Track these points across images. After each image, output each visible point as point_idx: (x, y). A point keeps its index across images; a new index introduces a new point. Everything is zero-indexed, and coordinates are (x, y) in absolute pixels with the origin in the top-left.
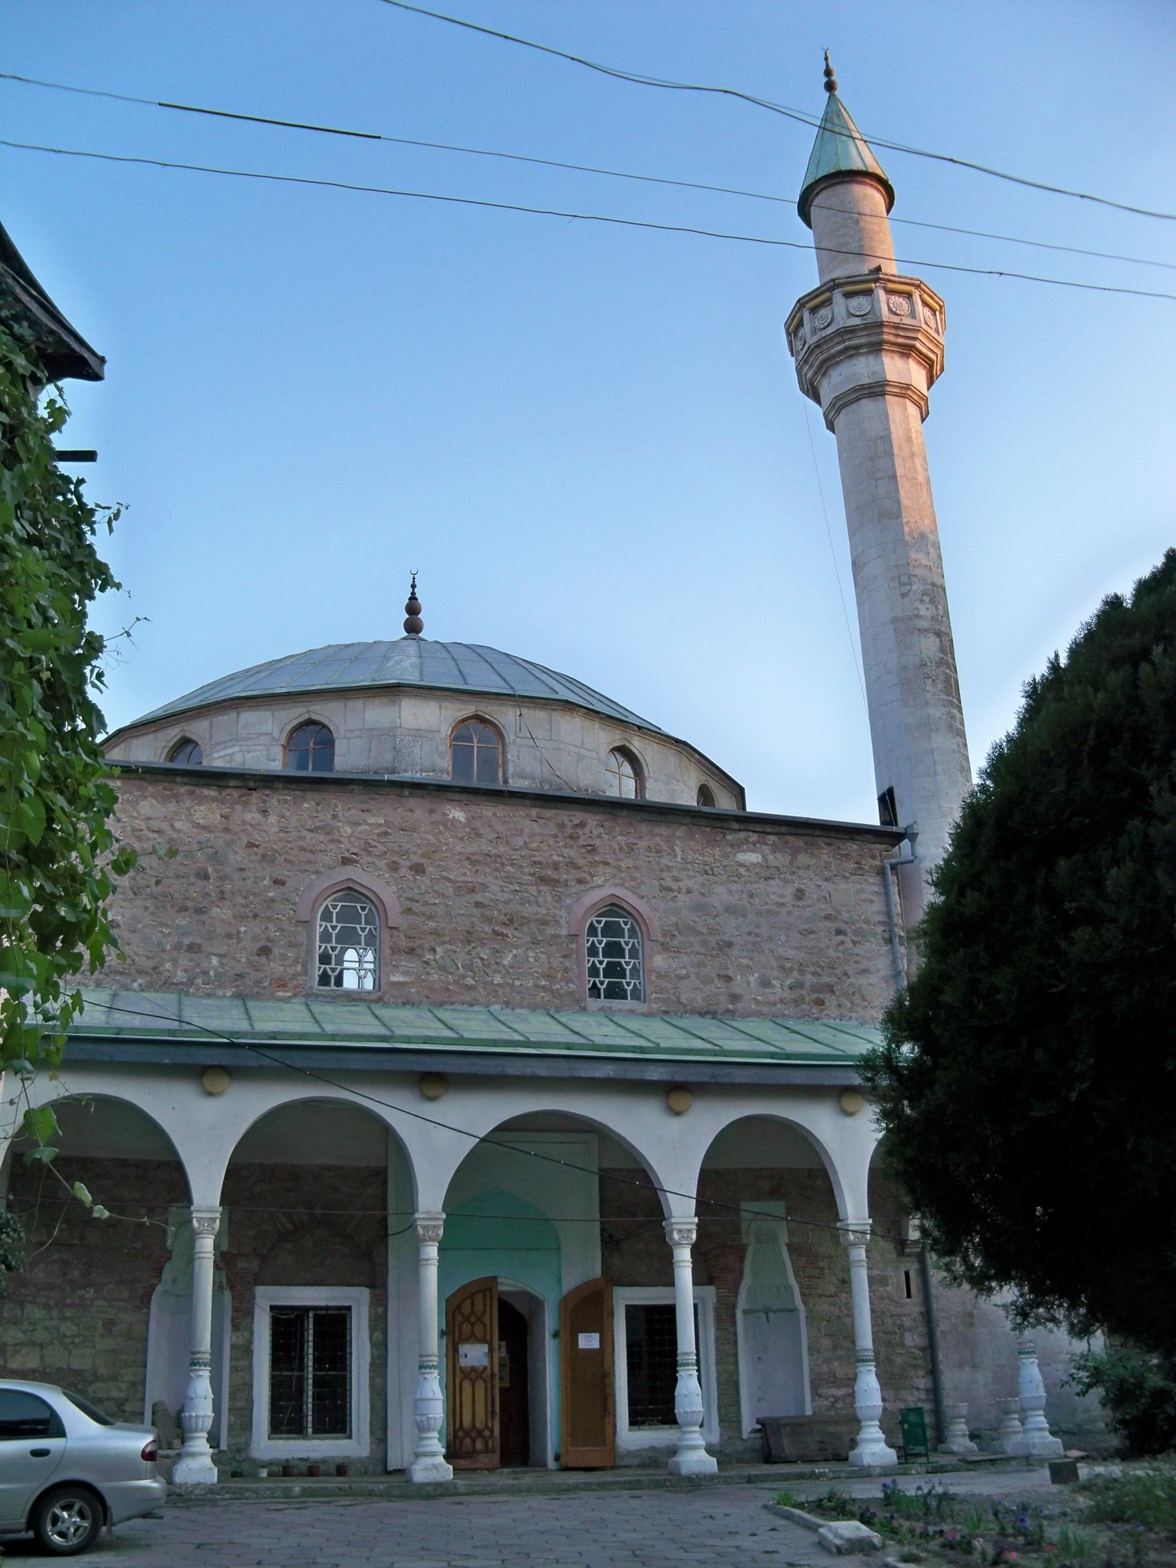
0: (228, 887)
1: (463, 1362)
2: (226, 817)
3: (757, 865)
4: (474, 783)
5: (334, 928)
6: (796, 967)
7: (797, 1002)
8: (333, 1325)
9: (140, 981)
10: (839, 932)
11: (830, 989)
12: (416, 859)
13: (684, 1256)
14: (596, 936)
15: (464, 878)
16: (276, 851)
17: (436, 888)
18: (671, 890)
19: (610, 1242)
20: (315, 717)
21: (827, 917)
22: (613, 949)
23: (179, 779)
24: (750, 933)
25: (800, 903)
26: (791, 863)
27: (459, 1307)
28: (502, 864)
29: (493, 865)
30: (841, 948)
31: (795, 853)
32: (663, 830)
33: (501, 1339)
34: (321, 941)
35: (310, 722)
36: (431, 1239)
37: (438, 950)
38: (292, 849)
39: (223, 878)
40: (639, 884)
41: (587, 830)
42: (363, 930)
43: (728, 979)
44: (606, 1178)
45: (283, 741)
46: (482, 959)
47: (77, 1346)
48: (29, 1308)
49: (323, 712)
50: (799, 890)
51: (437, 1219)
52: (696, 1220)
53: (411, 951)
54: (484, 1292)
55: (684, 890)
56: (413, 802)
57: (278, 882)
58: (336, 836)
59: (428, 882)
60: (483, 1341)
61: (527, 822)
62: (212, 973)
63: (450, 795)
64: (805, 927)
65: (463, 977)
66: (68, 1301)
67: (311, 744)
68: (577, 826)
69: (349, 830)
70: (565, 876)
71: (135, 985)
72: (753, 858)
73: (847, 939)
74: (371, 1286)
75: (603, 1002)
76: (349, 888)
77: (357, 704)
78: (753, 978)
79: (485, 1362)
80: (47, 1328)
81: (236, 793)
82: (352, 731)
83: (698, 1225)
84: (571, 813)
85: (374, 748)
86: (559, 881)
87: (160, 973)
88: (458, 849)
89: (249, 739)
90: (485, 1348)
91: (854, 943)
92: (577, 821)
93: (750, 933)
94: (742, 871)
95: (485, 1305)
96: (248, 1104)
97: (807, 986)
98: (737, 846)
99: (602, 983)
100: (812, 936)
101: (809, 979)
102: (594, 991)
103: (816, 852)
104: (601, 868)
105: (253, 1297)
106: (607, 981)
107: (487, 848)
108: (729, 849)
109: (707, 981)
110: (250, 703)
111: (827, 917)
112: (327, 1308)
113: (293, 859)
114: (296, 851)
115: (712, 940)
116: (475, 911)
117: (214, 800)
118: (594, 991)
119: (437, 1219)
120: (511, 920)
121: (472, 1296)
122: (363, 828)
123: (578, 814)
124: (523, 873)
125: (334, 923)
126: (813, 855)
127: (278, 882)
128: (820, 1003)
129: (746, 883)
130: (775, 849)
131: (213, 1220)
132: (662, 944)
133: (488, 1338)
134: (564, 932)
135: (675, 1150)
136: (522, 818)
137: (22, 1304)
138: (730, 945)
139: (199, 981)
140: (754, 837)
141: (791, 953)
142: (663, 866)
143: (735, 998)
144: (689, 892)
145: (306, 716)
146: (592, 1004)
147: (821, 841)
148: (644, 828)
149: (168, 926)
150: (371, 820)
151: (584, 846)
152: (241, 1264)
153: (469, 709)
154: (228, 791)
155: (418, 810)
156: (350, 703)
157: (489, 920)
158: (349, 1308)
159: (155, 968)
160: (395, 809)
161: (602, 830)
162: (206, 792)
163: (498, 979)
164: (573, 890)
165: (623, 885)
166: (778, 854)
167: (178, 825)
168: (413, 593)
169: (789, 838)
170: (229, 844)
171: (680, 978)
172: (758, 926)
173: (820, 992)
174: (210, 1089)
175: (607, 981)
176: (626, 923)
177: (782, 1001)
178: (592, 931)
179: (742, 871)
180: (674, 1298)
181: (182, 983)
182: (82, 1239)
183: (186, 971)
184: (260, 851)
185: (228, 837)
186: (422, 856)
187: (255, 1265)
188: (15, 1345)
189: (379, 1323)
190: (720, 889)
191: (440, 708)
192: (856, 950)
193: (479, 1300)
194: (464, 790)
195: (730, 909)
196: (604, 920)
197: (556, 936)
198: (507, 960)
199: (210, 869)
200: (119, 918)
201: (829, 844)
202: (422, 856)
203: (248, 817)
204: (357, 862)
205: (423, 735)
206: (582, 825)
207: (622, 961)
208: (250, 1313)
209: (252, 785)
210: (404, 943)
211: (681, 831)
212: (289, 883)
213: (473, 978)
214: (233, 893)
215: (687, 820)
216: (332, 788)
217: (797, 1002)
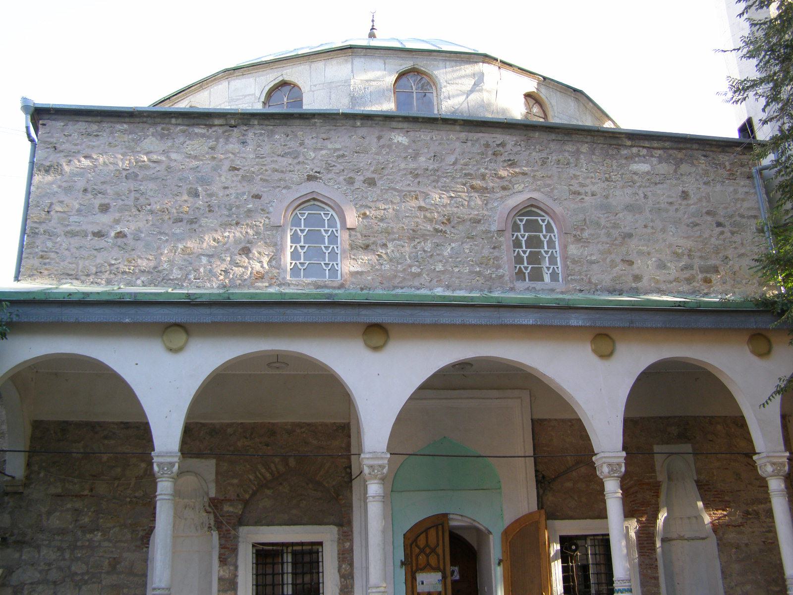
0: (214, 201)
1: (420, 588)
2: (212, 148)
3: (648, 173)
4: (414, 112)
5: (302, 231)
6: (686, 252)
7: (689, 280)
8: (307, 558)
9: (143, 278)
10: (719, 224)
11: (716, 270)
12: (369, 175)
13: (613, 491)
14: (520, 231)
15: (410, 189)
16: (253, 172)
17: (385, 196)
18: (579, 194)
19: (543, 482)
20: (287, 78)
21: (708, 213)
22: (534, 242)
23: (173, 121)
24: (646, 226)
25: (685, 202)
26: (675, 171)
27: (415, 540)
28: (438, 176)
29: (432, 178)
30: (721, 237)
31: (678, 163)
32: (570, 147)
33: (452, 564)
34: (292, 242)
35: (284, 84)
36: (375, 477)
37: (390, 245)
38: (266, 170)
39: (211, 195)
40: (552, 190)
41: (509, 147)
42: (326, 231)
43: (631, 263)
44: (538, 426)
45: (263, 99)
46: (424, 251)
47: (86, 583)
48: (44, 551)
49: (290, 74)
50: (683, 192)
51: (382, 458)
52: (624, 454)
53: (366, 247)
54: (436, 526)
55: (590, 194)
56: (363, 131)
57: (257, 197)
58: (301, 159)
59: (379, 192)
60: (436, 569)
61: (458, 144)
62: (202, 270)
63: (394, 124)
64: (691, 220)
65: (410, 266)
66: (79, 544)
67: (285, 99)
68: (498, 145)
69: (312, 155)
70: (491, 185)
71: (139, 282)
72: (644, 167)
73: (726, 230)
74: (339, 525)
75: (527, 283)
76: (314, 199)
77: (319, 65)
78: (652, 262)
79: (440, 588)
80: (60, 569)
81: (220, 130)
82: (315, 86)
83: (625, 459)
84: (494, 135)
85: (333, 96)
86: (486, 189)
87: (159, 271)
88: (403, 166)
89: (238, 99)
90: (438, 576)
91: (733, 233)
92: (498, 142)
93: (646, 226)
94: (636, 178)
95: (438, 541)
96: (206, 358)
97: (696, 267)
98: (630, 158)
99: (526, 268)
100: (697, 228)
101: (697, 263)
102: (520, 275)
103: (695, 162)
104: (520, 177)
105: (236, 537)
106: (530, 266)
107: (424, 165)
108: (624, 161)
109: (613, 264)
110: (237, 73)
111: (708, 213)
112: (302, 544)
113: (267, 178)
114: (269, 172)
115: (615, 233)
116: (421, 214)
117: (203, 136)
118: (520, 275)
119: (382, 458)
120: (449, 220)
121: (426, 531)
122: (324, 152)
123: (498, 136)
124: (457, 183)
125: (303, 228)
126: (693, 164)
127: (257, 197)
128: (707, 281)
129: (640, 187)
130: (661, 160)
131: (172, 464)
132: (575, 236)
133: (442, 567)
134: (494, 228)
135: (598, 390)
136: (454, 137)
137: (38, 548)
138: (630, 236)
139: (192, 277)
140: (644, 152)
141: (681, 242)
142: (571, 175)
143: (637, 278)
144: (593, 195)
145: (280, 79)
146: (520, 285)
147: (698, 154)
148: (552, 145)
149: (166, 234)
150: (330, 146)
151: (505, 161)
152: (227, 508)
153: (407, 64)
154: (214, 129)
155: (370, 136)
156: (314, 65)
157: (431, 220)
158: (321, 544)
159: (155, 268)
160: (350, 137)
161: (519, 148)
162: (197, 130)
163: (439, 267)
164: (499, 195)
165: (539, 190)
166: (664, 165)
167: (174, 156)
168: (373, 26)
169: (671, 152)
170: (215, 169)
171: (592, 262)
172: (652, 221)
173: (707, 272)
174: (174, 347)
175: (530, 266)
176: (543, 221)
177: (676, 280)
178: (516, 228)
179: (636, 178)
180: (608, 529)
181: (177, 279)
182: (91, 490)
183: (181, 269)
184: (241, 172)
185: (214, 163)
186: (373, 172)
187: (238, 509)
188: (32, 584)
189: (346, 557)
190: (618, 193)
191: (385, 64)
192: (734, 239)
193: (432, 532)
194: (406, 119)
195: (629, 208)
196: (525, 218)
197: (488, 232)
198: (447, 252)
199: (200, 189)
200: (126, 230)
201: (705, 156)
202: (373, 172)
203: (230, 147)
204: (320, 178)
205: (373, 86)
206: (502, 145)
207: (541, 235)
208: (234, 550)
209: (233, 122)
210: (360, 241)
211: (585, 148)
212: (265, 196)
213: (419, 267)
214: (219, 207)
215: (589, 139)
216: (297, 122)
217: (689, 280)
